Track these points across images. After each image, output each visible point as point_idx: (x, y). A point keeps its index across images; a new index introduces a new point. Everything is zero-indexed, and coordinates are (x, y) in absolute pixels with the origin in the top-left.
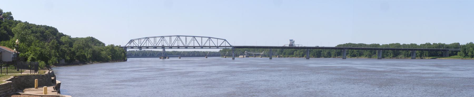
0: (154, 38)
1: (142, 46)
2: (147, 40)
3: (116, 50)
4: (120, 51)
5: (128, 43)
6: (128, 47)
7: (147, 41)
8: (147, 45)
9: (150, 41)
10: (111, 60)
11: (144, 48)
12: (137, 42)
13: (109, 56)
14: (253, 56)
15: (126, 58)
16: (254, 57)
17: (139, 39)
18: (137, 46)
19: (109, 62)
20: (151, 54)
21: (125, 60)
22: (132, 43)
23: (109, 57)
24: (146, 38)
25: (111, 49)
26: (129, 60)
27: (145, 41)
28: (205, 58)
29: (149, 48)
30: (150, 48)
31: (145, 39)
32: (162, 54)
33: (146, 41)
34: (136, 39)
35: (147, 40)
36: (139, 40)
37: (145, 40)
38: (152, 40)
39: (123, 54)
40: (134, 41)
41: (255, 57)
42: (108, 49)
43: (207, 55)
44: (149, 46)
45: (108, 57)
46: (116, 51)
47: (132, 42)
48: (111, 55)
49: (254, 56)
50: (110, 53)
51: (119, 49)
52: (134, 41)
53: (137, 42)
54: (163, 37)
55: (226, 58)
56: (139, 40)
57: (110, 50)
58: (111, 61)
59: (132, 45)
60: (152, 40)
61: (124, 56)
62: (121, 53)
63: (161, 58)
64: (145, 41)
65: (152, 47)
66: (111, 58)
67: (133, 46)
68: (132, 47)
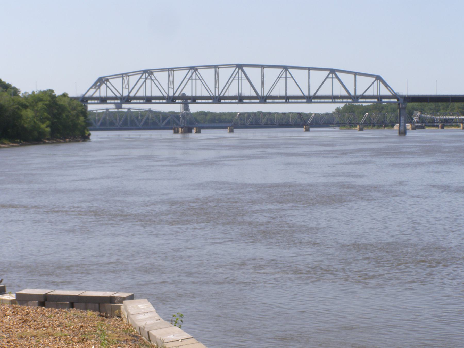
0: (167, 72)
1: (132, 95)
2: (146, 78)
3: (62, 105)
4: (74, 109)
5: (91, 88)
6: (91, 98)
7: (148, 82)
8: (148, 94)
9: (156, 81)
10: (49, 137)
11: (138, 101)
12: (117, 83)
13: (43, 123)
14: (437, 126)
15: (86, 132)
16: (440, 128)
17: (123, 75)
18: (118, 95)
19: (45, 143)
20: (148, 118)
21: (86, 138)
22: (103, 87)
23: (43, 126)
24: (145, 72)
25: (47, 102)
26: (95, 136)
27: (142, 81)
28: (303, 132)
29: (153, 101)
30: (158, 101)
31: (143, 74)
32: (181, 120)
33: (145, 81)
34: (116, 76)
35: (146, 78)
36: (123, 77)
37: (140, 78)
38: (162, 77)
39: (82, 118)
40: (107, 80)
41: (443, 127)
42: (40, 104)
43: (309, 122)
44: (154, 94)
45: (39, 127)
46: (62, 109)
47: (104, 82)
48: (48, 122)
49: (440, 125)
50: (46, 114)
51: (70, 105)
52: (107, 80)
53: (117, 83)
54: (194, 69)
55: (361, 132)
56: (123, 77)
57: (46, 105)
58: (48, 139)
59: (103, 92)
60: (162, 77)
61: (83, 124)
62: (77, 116)
63: (176, 132)
64: (142, 81)
65: (163, 98)
66: (48, 129)
67: (105, 95)
68: (103, 100)
